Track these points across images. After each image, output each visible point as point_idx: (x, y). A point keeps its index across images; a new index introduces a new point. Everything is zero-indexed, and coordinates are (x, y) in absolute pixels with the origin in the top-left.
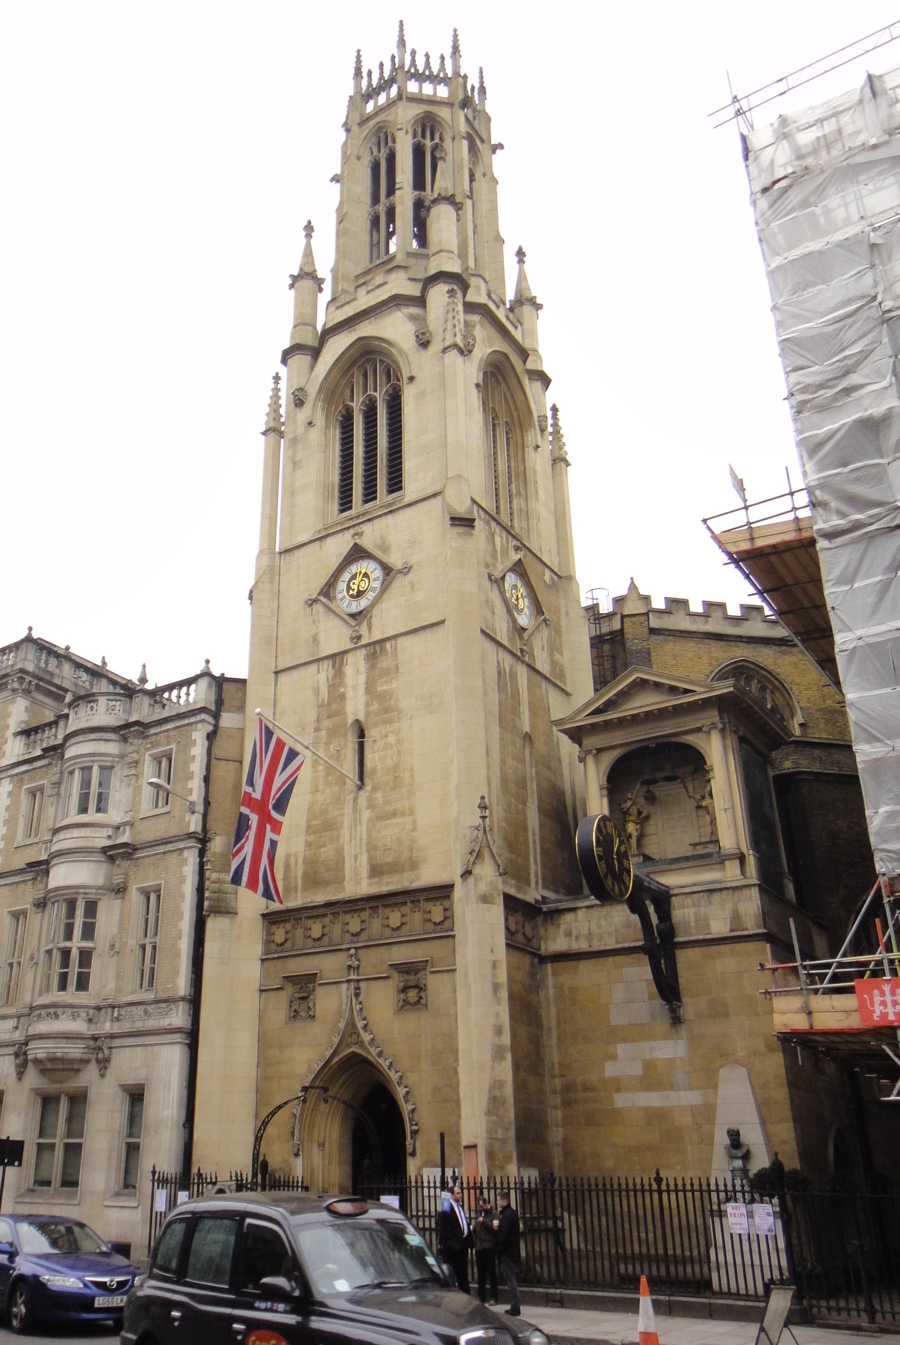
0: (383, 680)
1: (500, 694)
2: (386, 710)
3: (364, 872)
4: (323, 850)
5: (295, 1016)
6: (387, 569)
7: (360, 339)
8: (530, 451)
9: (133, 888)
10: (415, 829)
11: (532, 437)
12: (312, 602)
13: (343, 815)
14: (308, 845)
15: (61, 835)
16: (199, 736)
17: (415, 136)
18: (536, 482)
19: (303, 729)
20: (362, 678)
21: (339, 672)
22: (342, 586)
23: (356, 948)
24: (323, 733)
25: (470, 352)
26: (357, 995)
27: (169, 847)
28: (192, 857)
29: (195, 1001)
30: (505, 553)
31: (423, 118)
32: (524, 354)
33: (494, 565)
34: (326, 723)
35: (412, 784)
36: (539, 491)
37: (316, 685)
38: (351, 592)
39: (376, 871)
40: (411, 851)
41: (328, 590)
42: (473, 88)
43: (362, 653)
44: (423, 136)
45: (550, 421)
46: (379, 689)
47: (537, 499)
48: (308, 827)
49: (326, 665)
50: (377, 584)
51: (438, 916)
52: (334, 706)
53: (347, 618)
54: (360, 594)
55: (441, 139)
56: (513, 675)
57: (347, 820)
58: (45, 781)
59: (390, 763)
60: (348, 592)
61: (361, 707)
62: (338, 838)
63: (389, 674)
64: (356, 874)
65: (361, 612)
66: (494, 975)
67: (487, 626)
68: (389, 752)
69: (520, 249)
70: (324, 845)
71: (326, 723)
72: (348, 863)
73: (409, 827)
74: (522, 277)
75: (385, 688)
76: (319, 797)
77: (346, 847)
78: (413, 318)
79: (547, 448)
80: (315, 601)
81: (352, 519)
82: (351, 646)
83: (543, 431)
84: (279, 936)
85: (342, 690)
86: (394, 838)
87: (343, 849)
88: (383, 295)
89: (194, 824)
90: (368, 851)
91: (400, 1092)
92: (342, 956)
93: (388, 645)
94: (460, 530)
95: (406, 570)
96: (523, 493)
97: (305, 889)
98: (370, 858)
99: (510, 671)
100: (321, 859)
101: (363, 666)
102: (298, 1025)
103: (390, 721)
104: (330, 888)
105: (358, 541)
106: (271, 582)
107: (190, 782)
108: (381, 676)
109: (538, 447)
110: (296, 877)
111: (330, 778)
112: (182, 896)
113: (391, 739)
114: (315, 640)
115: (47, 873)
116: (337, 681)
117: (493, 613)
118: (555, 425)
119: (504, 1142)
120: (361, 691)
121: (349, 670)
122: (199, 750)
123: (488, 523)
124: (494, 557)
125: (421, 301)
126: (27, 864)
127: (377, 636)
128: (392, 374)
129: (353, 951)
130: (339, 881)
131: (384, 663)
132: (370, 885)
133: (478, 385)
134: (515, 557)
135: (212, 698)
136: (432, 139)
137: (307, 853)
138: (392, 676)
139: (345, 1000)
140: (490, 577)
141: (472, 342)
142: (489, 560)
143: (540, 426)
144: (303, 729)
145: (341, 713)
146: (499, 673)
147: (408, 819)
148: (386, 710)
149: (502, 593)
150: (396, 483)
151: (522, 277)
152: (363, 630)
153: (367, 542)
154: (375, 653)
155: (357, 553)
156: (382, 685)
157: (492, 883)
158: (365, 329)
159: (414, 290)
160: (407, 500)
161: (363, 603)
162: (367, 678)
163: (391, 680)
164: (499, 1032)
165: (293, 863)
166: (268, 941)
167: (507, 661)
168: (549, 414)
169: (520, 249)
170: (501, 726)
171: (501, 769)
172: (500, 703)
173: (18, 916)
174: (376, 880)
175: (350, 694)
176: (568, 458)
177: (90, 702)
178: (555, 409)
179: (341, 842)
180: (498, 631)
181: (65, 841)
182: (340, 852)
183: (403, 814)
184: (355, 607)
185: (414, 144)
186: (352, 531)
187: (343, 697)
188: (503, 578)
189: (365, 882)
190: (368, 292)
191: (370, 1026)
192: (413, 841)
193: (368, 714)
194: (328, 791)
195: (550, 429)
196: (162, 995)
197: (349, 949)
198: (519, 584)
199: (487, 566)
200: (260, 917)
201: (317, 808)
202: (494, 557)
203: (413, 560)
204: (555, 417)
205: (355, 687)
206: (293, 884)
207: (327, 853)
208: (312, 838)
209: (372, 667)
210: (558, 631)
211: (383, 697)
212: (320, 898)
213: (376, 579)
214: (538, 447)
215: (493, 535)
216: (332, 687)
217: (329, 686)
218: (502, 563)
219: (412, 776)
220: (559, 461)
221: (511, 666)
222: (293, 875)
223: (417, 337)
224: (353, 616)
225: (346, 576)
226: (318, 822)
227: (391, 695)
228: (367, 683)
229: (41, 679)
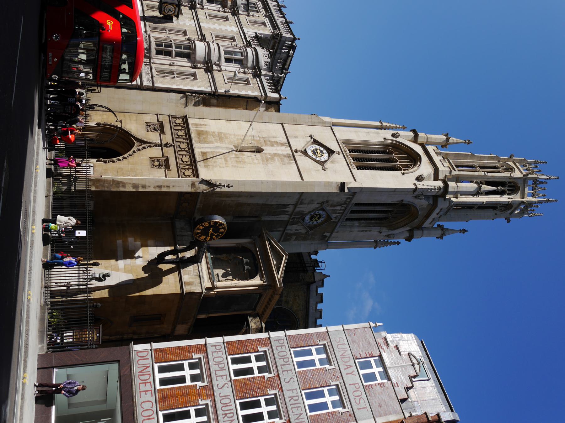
0: (279, 159)
1: (275, 205)
2: (267, 160)
3: (203, 150)
4: (212, 137)
5: (148, 125)
6: (325, 162)
7: (420, 157)
8: (378, 229)
9: (196, 70)
10: (220, 167)
11: (386, 231)
12: (311, 137)
13: (226, 144)
14: (214, 132)
15: (216, 46)
16: (256, 93)
17: (509, 183)
18: (366, 231)
19: (259, 132)
20: (280, 152)
21: (282, 145)
22: (318, 147)
23: (174, 146)
25: (416, 197)
26: (156, 146)
27: (212, 83)
28: (209, 89)
29: (153, 89)
30: (334, 211)
31: (518, 186)
32: (419, 227)
33: (328, 205)
34: (262, 140)
35: (238, 167)
36: (362, 233)
37: (277, 137)
38: (315, 150)
39: (204, 154)
40: (212, 166)
41: (316, 142)
43: (291, 153)
44: (509, 186)
45: (393, 241)
46: (276, 158)
47: (359, 231)
48: (221, 133)
49: (286, 141)
50: (318, 159)
51: (186, 173)
52: (269, 143)
53: (305, 148)
55: (508, 194)
56: (284, 213)
57: (224, 145)
58: (237, 42)
59: (246, 160)
60: (315, 149)
61: (268, 152)
62: (217, 142)
63: (282, 161)
64: (203, 148)
65: (307, 153)
66: (164, 186)
67: (302, 200)
68: (251, 160)
69: (467, 231)
70: (214, 137)
72: (206, 145)
73: (221, 165)
74: (454, 231)
75: (276, 160)
76: (233, 137)
77: (213, 144)
78: (429, 175)
79: (381, 237)
80: (311, 138)
81: (345, 151)
82: (293, 149)
83: (388, 236)
84: (179, 121)
85: (275, 146)
86: (217, 160)
87: (212, 143)
88: (439, 165)
89: (221, 90)
90: (212, 152)
91: (120, 158)
92: (171, 142)
93: (294, 161)
95: (324, 169)
96: (361, 226)
97: (197, 131)
98: (209, 152)
100: (208, 136)
101: (285, 153)
102: (144, 126)
103: (263, 161)
104: (197, 139)
105: (336, 153)
106: (319, 122)
107: (237, 90)
108: (281, 159)
109: (381, 233)
110: (201, 128)
111: (240, 140)
112: (193, 86)
113: (256, 161)
114: (296, 137)
115: (201, 40)
116: (279, 144)
117: (308, 204)
118: (391, 243)
119: (103, 186)
120: (275, 152)
121: (283, 148)
122: (250, 93)
123: (345, 203)
124: (332, 206)
125: (436, 178)
126: (204, 35)
127: (297, 158)
128: (406, 167)
129: (173, 145)
130: (200, 142)
131: (286, 160)
132: (199, 152)
133: (402, 201)
134: (334, 216)
135: (271, 100)
136: (508, 190)
137: (211, 132)
138: (281, 162)
139: (154, 142)
140: (323, 202)
141: (420, 198)
142: (330, 203)
143: (390, 235)
144: (259, 132)
145: (266, 145)
146: (284, 205)
147: (224, 165)
148: (267, 160)
149: (317, 209)
150: (359, 168)
151: (454, 231)
152: (299, 154)
153: (335, 156)
154: (290, 157)
155: (331, 152)
157: (199, 188)
158: (424, 158)
159: (441, 176)
160: (352, 170)
162: (281, 154)
164: (144, 187)
165: (206, 127)
166: (175, 117)
167: (290, 210)
168: (396, 241)
169: (467, 231)
170: (263, 204)
171: (246, 204)
172: (272, 205)
173: (185, 33)
174: (200, 154)
175: (274, 148)
176: (378, 248)
177: (269, 56)
178: (398, 243)
179: (215, 143)
180: (300, 206)
181: (214, 48)
182: (211, 142)
183: (226, 164)
184: (308, 151)
185: (506, 182)
186: (340, 151)
187: (272, 146)
188: (323, 209)
189: (200, 150)
190: (440, 160)
191: (144, 150)
192: (216, 166)
193: (265, 154)
194: (235, 139)
195: (389, 241)
196: (155, 79)
197: (173, 143)
198: (322, 219)
199: (327, 202)
200: (185, 115)
201: (228, 135)
202: (332, 206)
203: (327, 171)
204: (395, 243)
205: (276, 150)
206: (198, 127)
207: (211, 138)
208: (217, 134)
209: (285, 156)
210: (305, 239)
212: (193, 135)
213: (320, 159)
214: (381, 233)
215: (340, 205)
216: (277, 143)
219: (241, 167)
220: (376, 244)
221: (287, 212)
222: (202, 126)
223: (421, 175)
224: (305, 150)
225: (322, 149)
226: (223, 136)
228: (278, 154)
229: (279, 43)
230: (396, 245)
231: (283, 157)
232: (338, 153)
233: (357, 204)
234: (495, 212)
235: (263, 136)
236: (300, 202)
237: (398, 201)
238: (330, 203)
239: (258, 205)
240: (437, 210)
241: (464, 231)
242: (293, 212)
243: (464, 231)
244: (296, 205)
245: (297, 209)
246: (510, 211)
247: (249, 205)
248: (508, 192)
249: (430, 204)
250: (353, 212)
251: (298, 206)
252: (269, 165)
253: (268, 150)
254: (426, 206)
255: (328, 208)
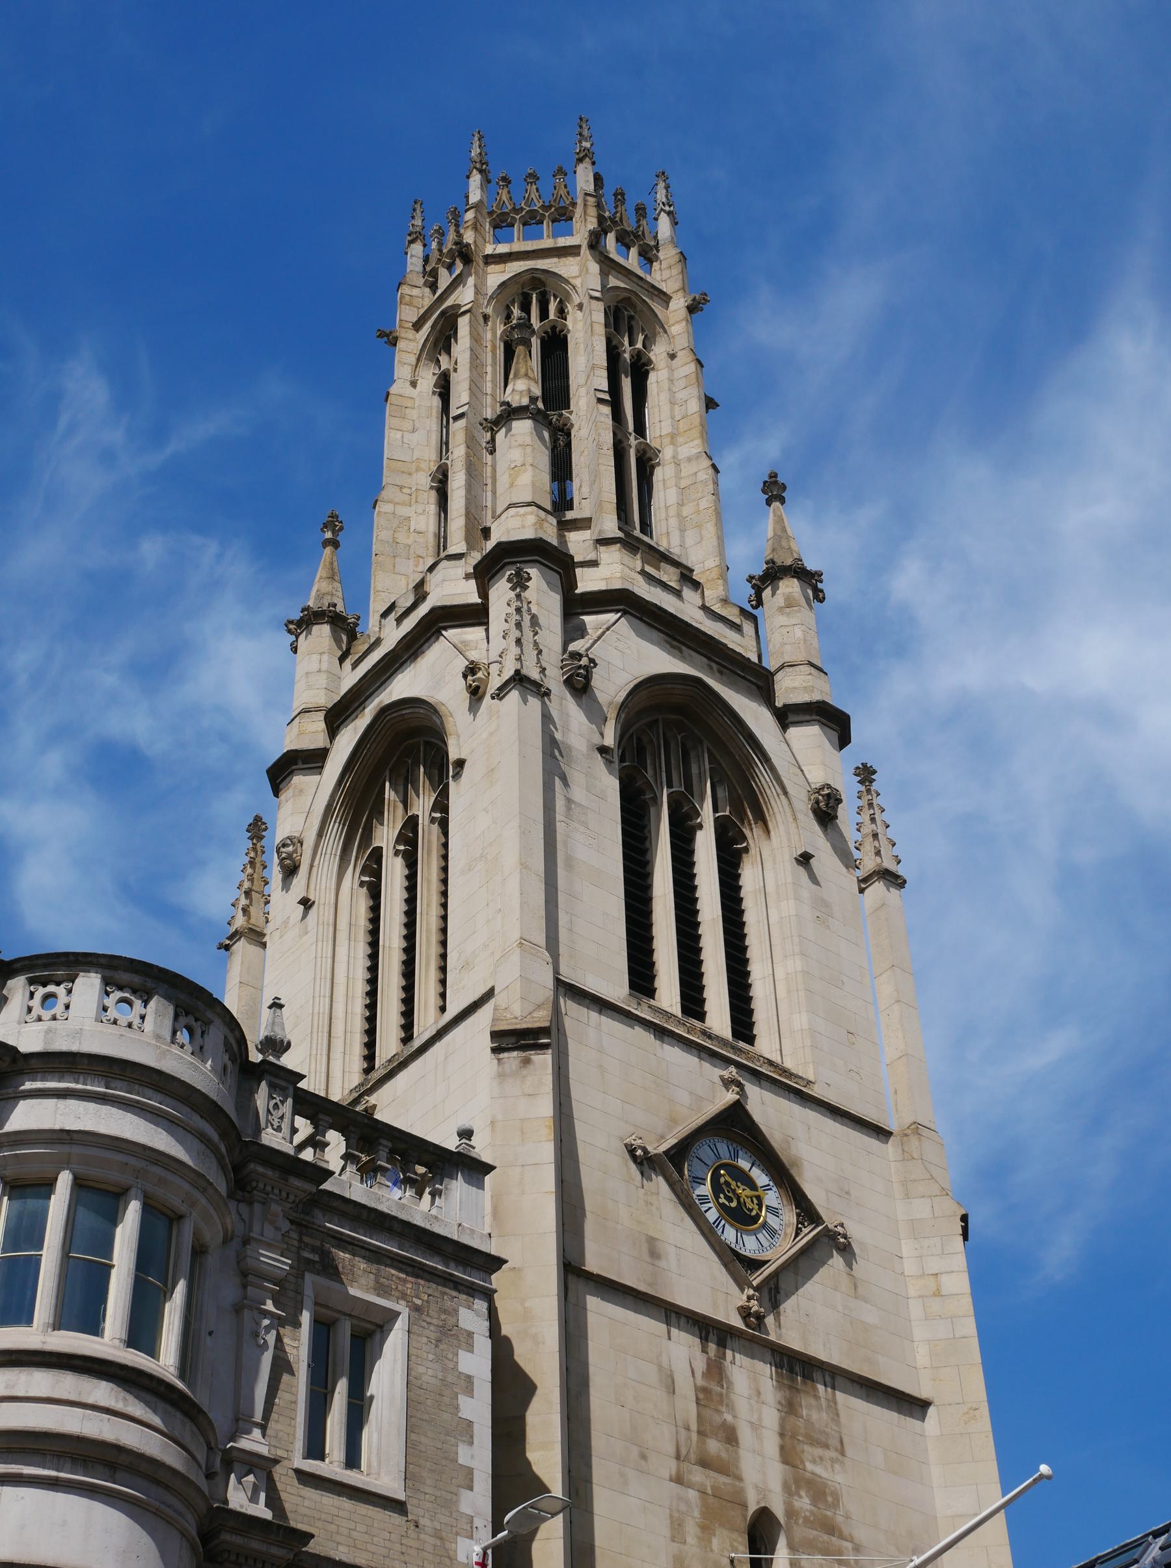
0: (818, 1451)
19: (644, 1457)
20: (771, 1417)
21: (716, 1371)
24: (692, 1494)
46: (809, 1466)
54: (743, 1218)
71: (698, 1476)
82: (737, 1322)
85: (729, 1418)
148: (831, 1529)
156: (814, 1462)
161: (750, 1246)
162: (782, 1426)
163: (833, 1461)
175: (745, 1435)
187: (731, 1437)
193: (791, 1513)
211: (820, 1492)
217: (697, 1389)
227: (837, 1497)
228: (782, 1435)
231: (800, 1423)
235: (671, 1450)
252: (861, 1534)
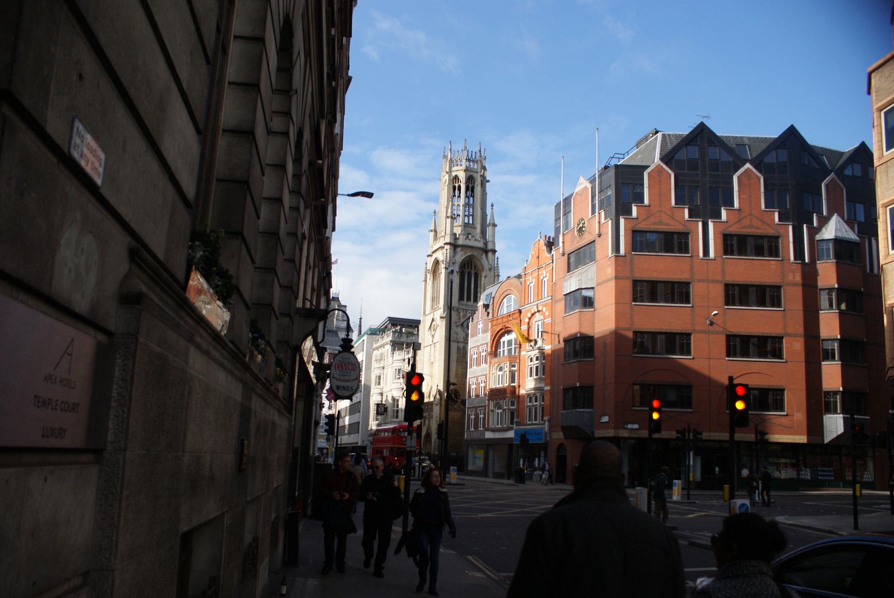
8: (483, 279)
30: (464, 316)
42: (476, 153)
44: (456, 183)
55: (461, 182)
69: (492, 204)
94: (442, 319)
99: (463, 347)
118: (498, 264)
136: (458, 183)
142: (457, 321)
159: (443, 245)
168: (496, 260)
169: (492, 204)
171: (456, 373)
172: (457, 357)
178: (498, 258)
202: (460, 318)
204: (497, 262)
215: (459, 313)
218: (463, 319)
230: (499, 260)
232: (434, 315)
233: (461, 298)
234: (476, 186)
236: (456, 340)
237: (458, 275)
238: (457, 321)
239: (457, 365)
240: (468, 243)
241: (492, 206)
242: (463, 342)
243: (492, 206)
244: (458, 342)
245: (462, 340)
246: (475, 175)
247: (457, 371)
248: (459, 183)
249: (461, 250)
250: (469, 299)
251: (459, 340)
253: (432, 360)
254: (463, 252)
255: (462, 321)
